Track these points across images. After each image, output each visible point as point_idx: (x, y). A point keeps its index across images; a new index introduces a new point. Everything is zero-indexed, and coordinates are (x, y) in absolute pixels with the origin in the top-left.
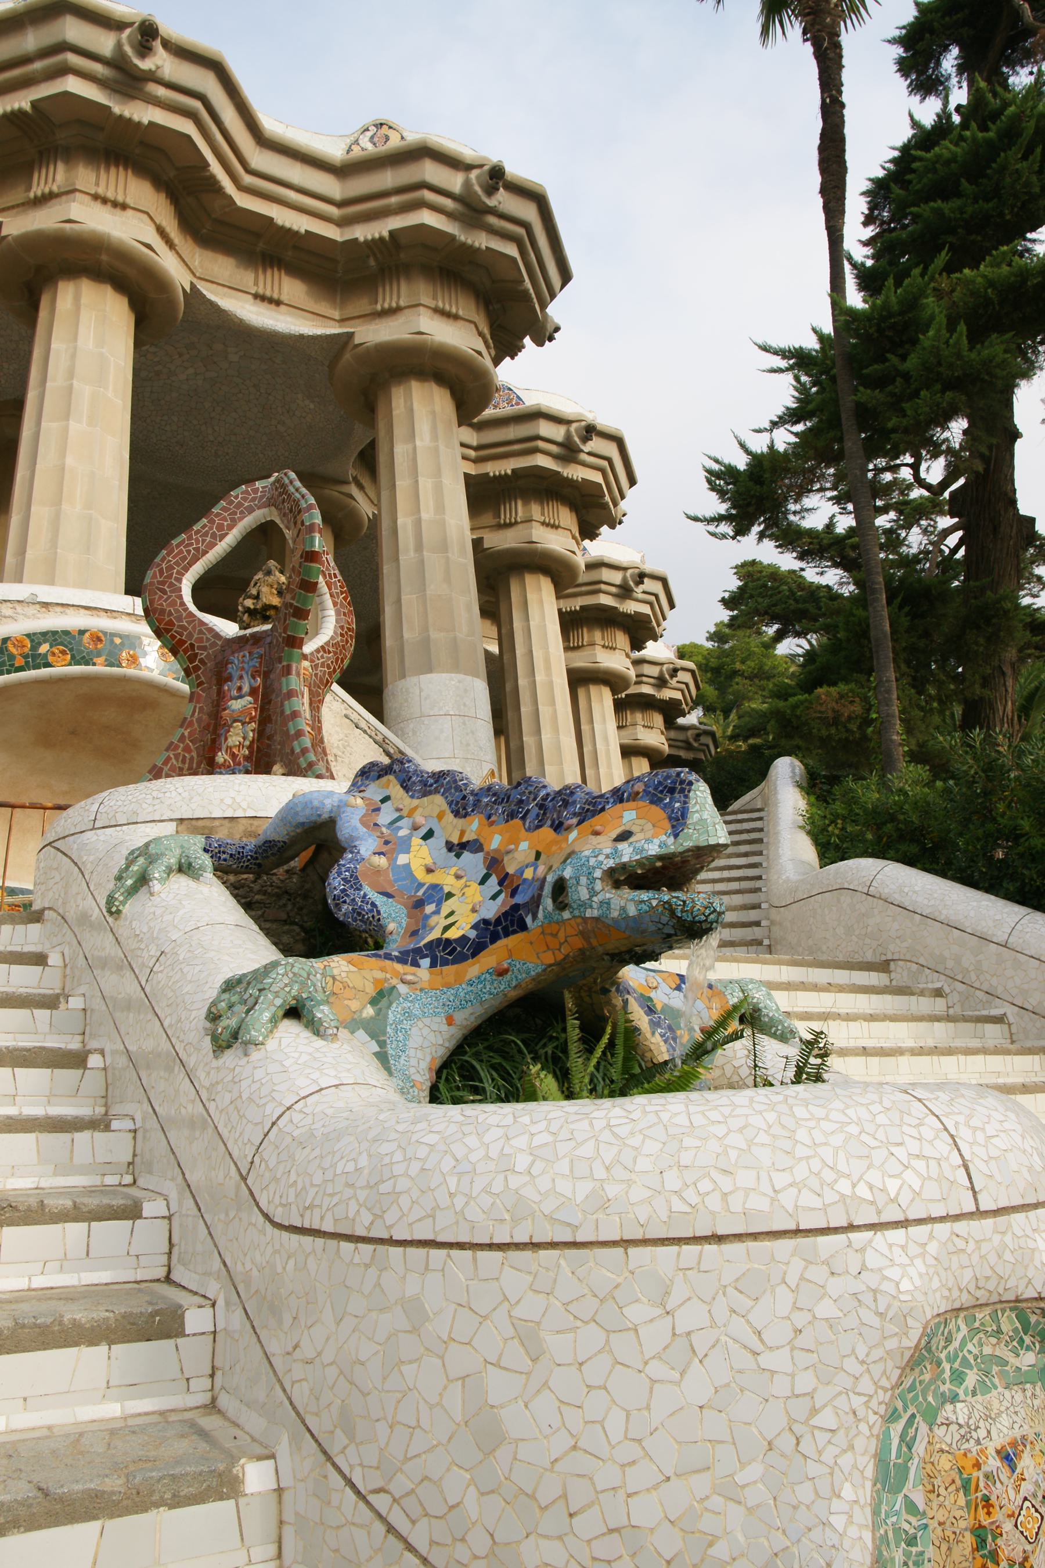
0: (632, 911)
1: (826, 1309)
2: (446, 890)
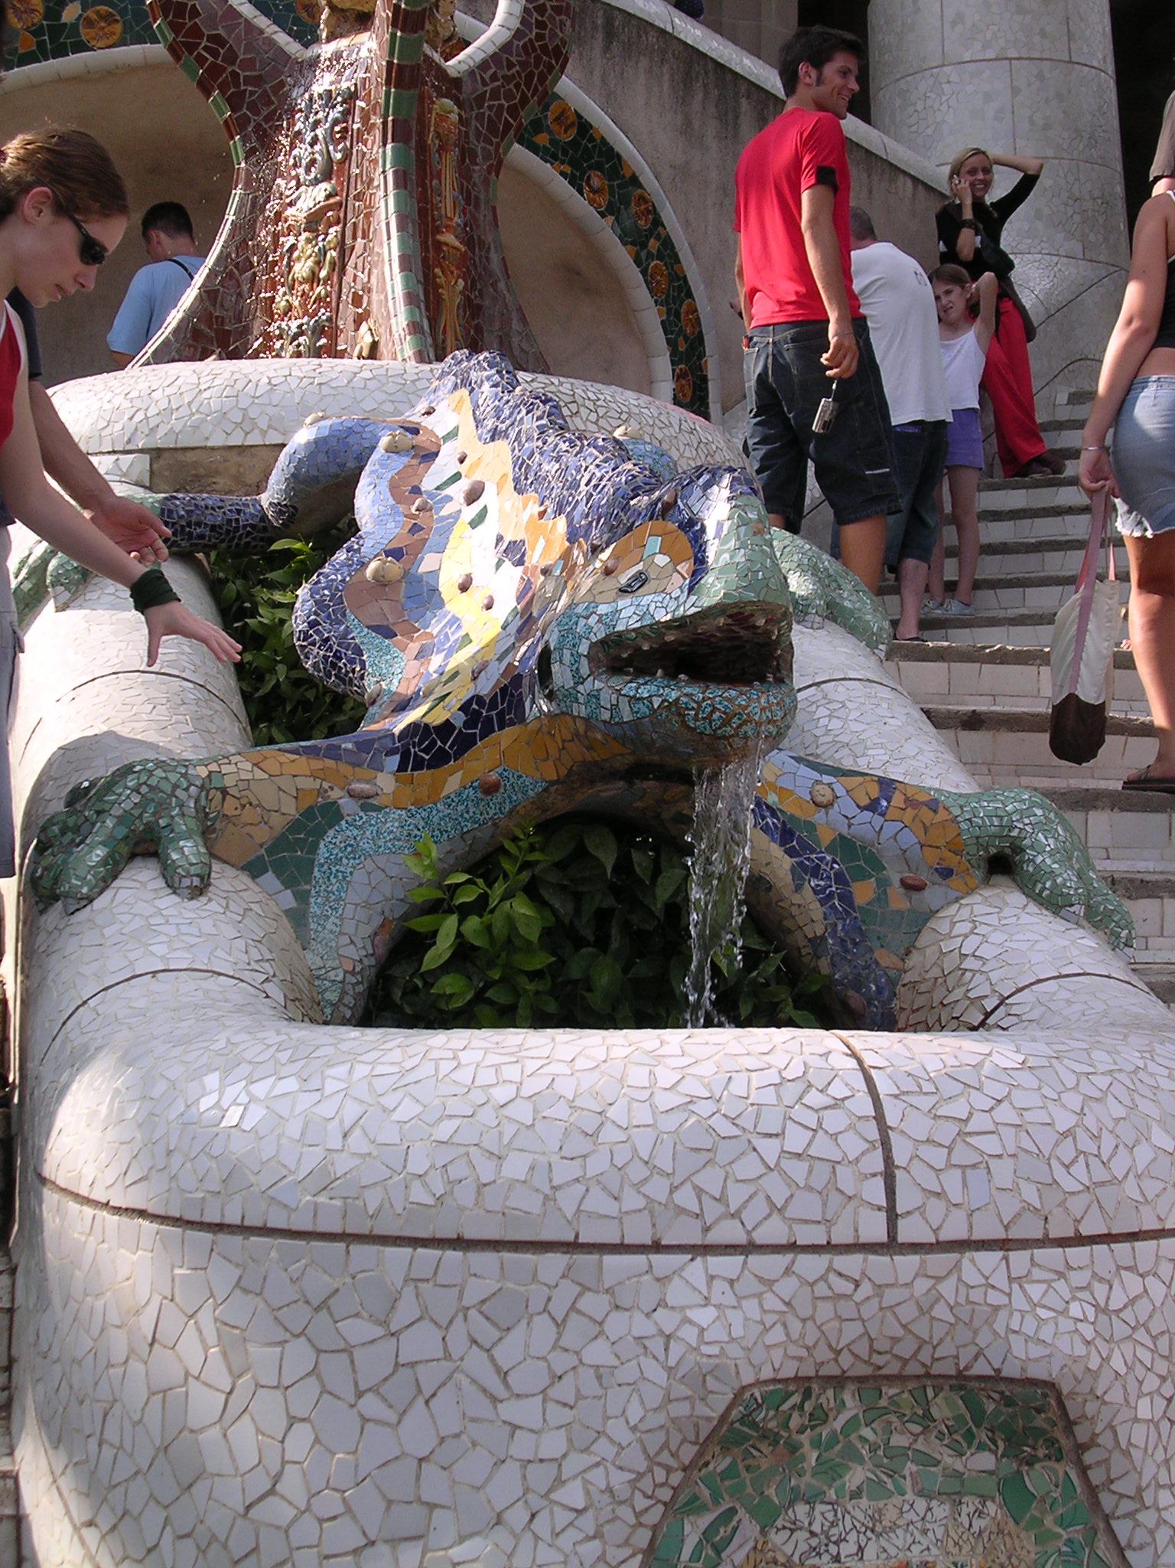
1: (598, 1353)
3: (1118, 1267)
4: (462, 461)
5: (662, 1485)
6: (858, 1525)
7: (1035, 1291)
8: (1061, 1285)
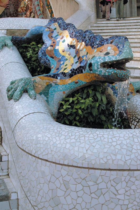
0: (107, 74)
1: (134, 187)
2: (66, 58)
4: (58, 33)
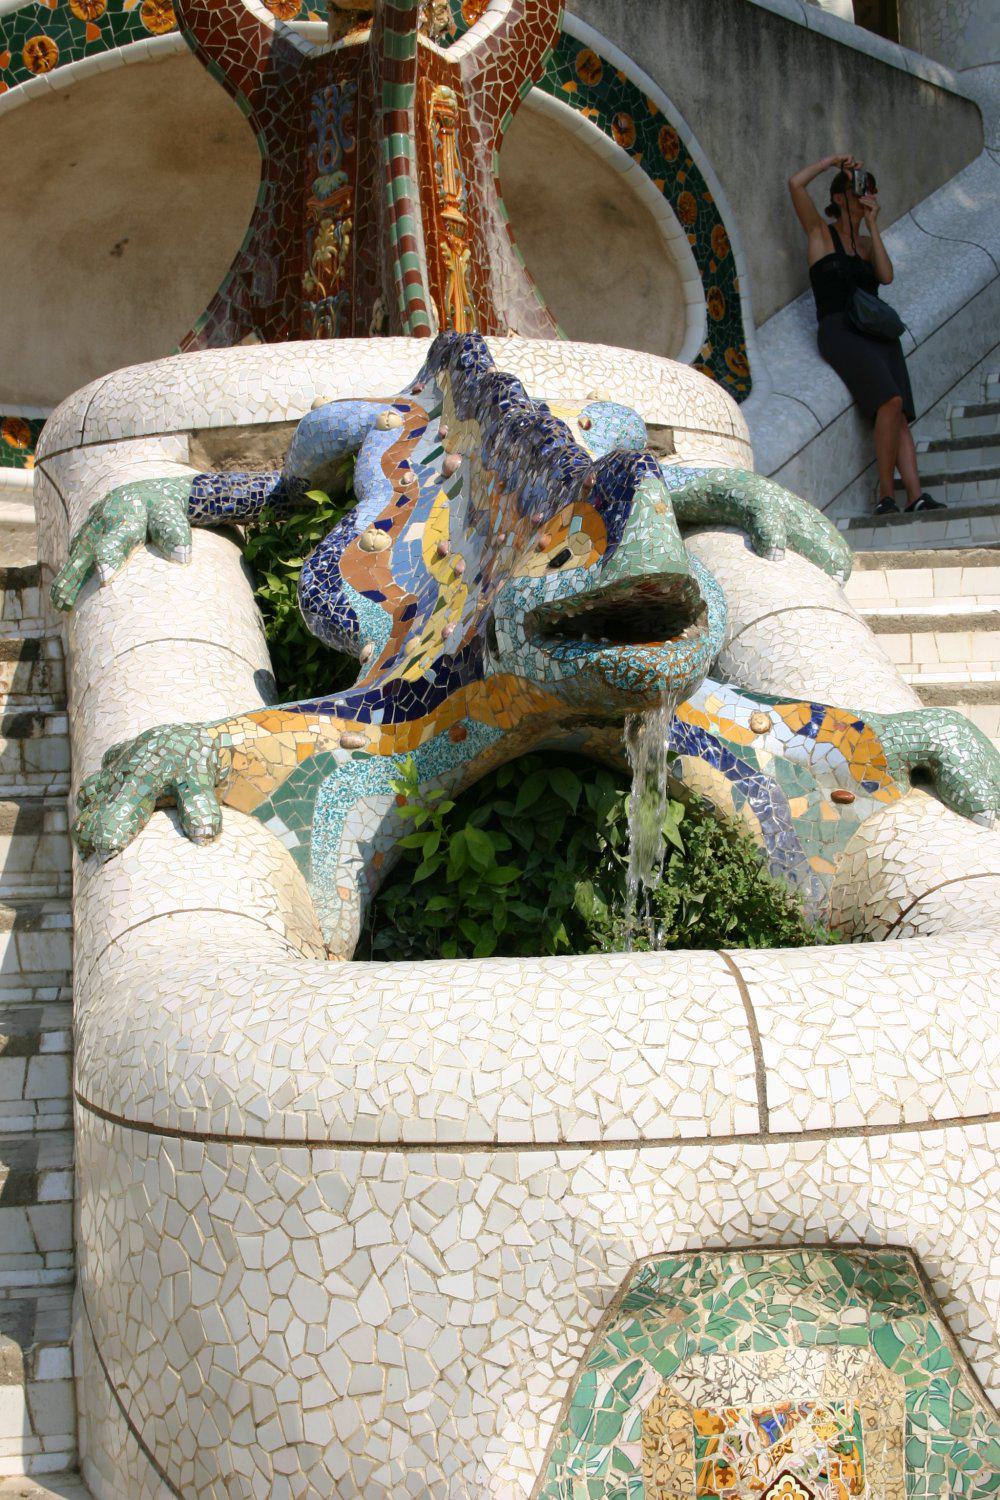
1: (518, 1235)
3: (971, 1146)
5: (575, 1344)
6: (747, 1373)
7: (893, 1170)
8: (917, 1164)
